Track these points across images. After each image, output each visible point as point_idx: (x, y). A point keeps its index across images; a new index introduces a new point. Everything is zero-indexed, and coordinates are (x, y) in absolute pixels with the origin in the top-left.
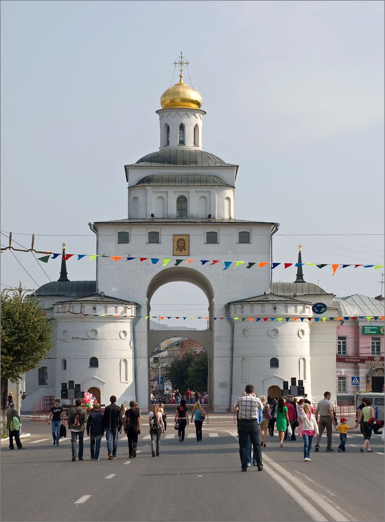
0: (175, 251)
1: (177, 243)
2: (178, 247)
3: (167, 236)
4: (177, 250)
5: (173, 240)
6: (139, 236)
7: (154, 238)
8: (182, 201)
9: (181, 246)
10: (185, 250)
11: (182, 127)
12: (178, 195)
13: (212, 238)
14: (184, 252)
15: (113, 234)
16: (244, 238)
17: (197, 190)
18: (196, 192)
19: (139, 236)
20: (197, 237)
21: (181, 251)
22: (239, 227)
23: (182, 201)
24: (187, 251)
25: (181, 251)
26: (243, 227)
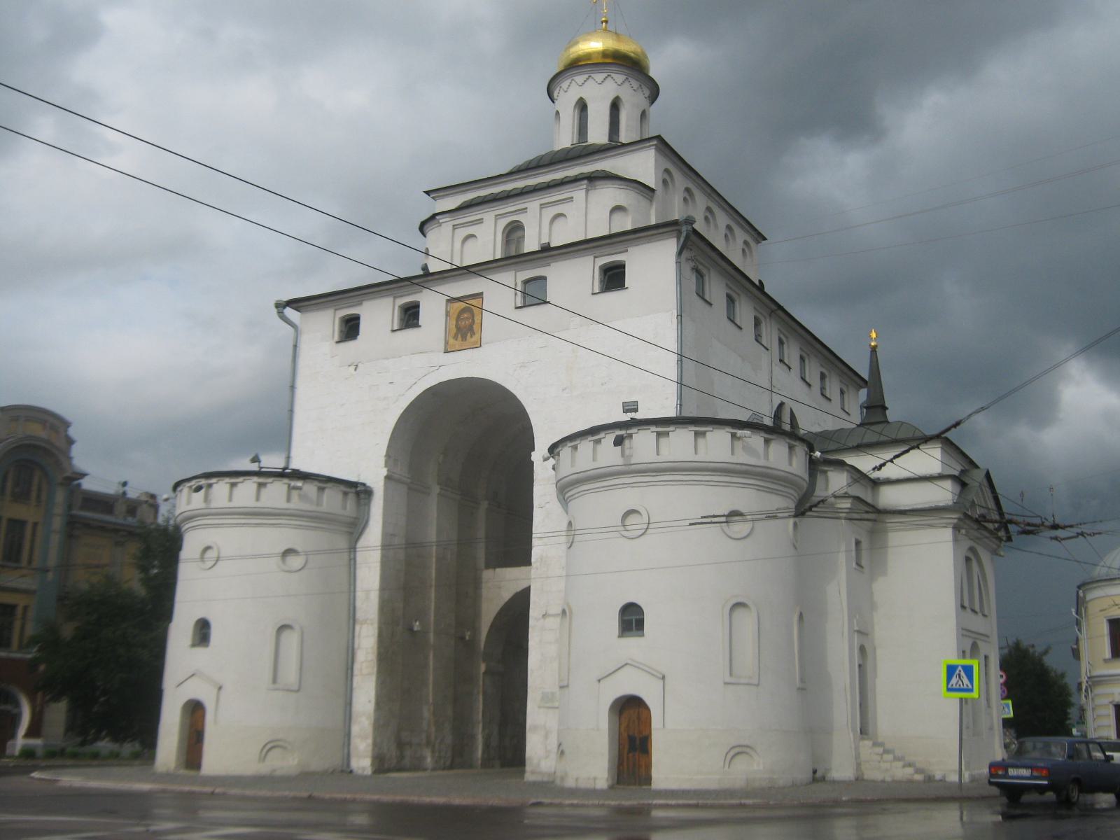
0: (452, 341)
1: (457, 321)
2: (458, 329)
3: (432, 304)
4: (455, 338)
5: (447, 314)
6: (378, 316)
7: (410, 316)
8: (514, 231)
9: (465, 326)
10: (473, 334)
11: (582, 106)
12: (503, 223)
13: (534, 294)
14: (470, 340)
15: (325, 323)
16: (613, 278)
17: (543, 201)
18: (542, 206)
19: (378, 316)
20: (498, 294)
21: (464, 338)
22: (597, 252)
23: (514, 231)
24: (477, 336)
25: (464, 338)
26: (608, 250)
